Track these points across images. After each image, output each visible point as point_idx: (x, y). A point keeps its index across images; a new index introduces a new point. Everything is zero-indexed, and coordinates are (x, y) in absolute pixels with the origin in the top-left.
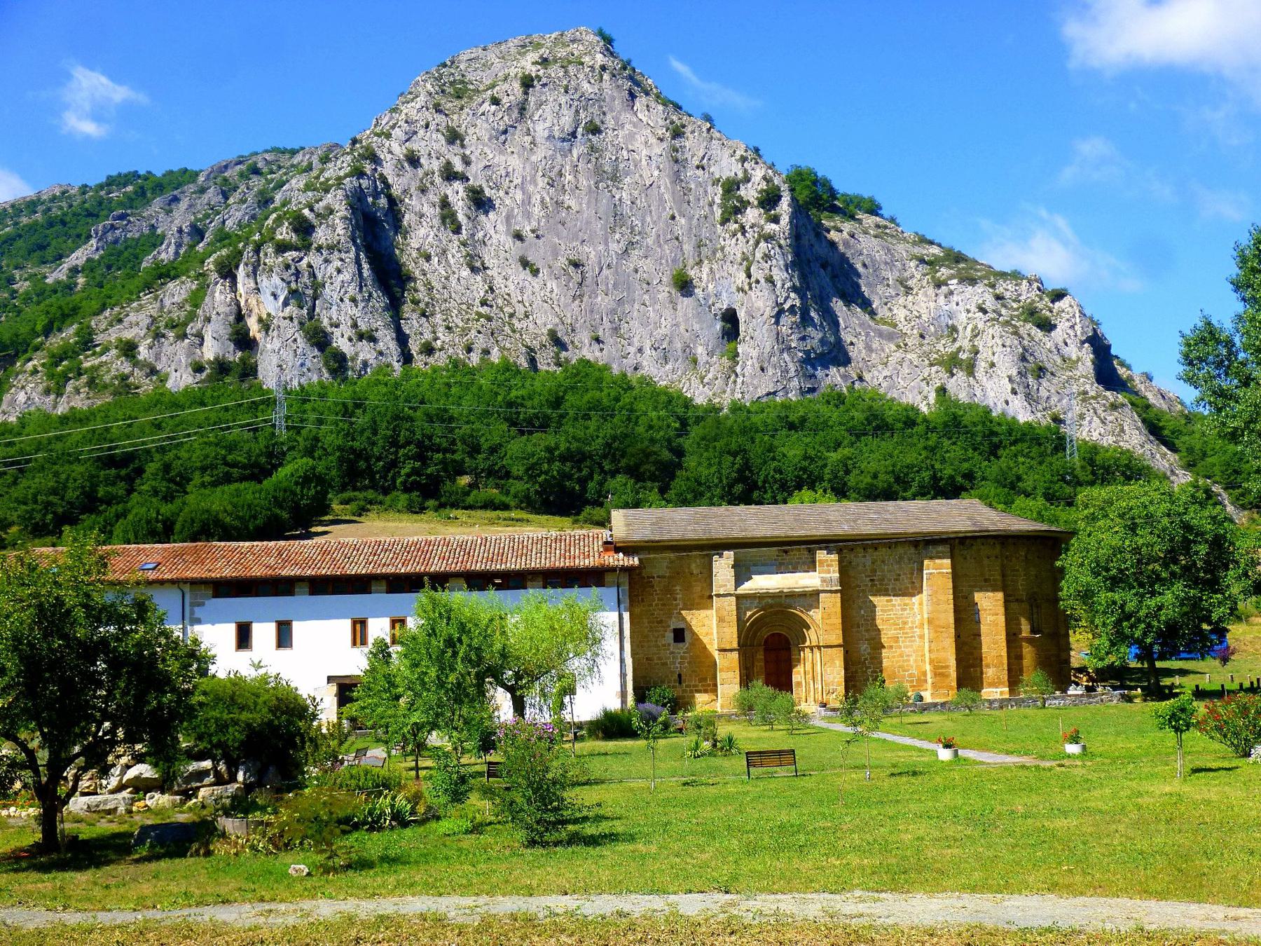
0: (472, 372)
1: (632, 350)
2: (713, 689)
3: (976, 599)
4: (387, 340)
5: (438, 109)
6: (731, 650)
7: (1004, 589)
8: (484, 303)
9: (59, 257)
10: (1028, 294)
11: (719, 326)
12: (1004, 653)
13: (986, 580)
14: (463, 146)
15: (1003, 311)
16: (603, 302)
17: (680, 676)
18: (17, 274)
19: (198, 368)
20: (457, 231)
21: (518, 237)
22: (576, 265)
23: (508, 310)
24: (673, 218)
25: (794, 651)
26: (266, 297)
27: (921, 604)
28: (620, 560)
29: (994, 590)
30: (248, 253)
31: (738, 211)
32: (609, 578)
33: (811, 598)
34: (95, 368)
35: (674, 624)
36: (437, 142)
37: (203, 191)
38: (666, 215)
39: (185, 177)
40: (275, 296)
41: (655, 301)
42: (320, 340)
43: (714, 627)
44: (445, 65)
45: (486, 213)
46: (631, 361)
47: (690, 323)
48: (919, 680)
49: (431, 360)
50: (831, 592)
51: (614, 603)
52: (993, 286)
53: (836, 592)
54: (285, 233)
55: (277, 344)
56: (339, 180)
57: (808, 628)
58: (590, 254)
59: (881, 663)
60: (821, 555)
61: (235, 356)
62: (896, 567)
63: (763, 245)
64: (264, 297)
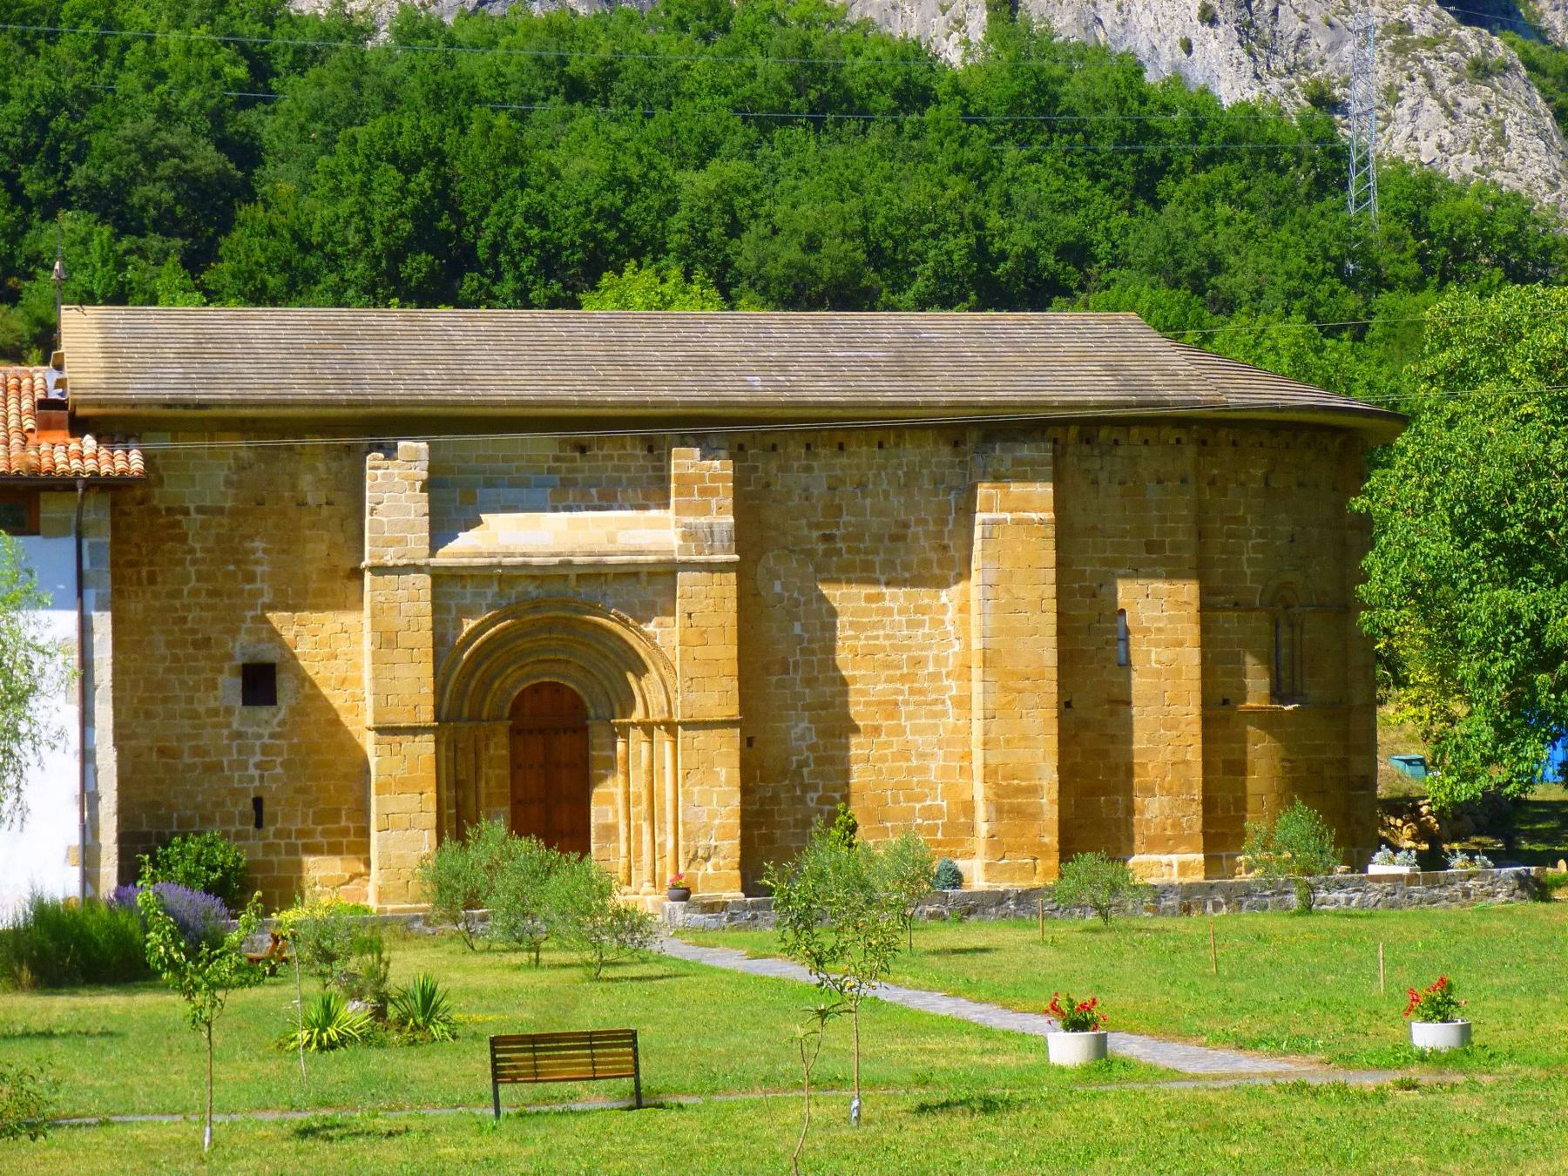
2: (358, 845)
3: (1123, 599)
6: (414, 731)
7: (1200, 572)
12: (1194, 755)
13: (1150, 547)
17: (258, 803)
25: (597, 736)
27: (964, 609)
28: (83, 455)
29: (1170, 576)
32: (52, 508)
33: (650, 583)
35: (242, 647)
43: (363, 661)
48: (950, 827)
50: (710, 567)
51: (68, 585)
53: (724, 567)
57: (641, 669)
59: (847, 774)
60: (685, 461)
62: (897, 502)
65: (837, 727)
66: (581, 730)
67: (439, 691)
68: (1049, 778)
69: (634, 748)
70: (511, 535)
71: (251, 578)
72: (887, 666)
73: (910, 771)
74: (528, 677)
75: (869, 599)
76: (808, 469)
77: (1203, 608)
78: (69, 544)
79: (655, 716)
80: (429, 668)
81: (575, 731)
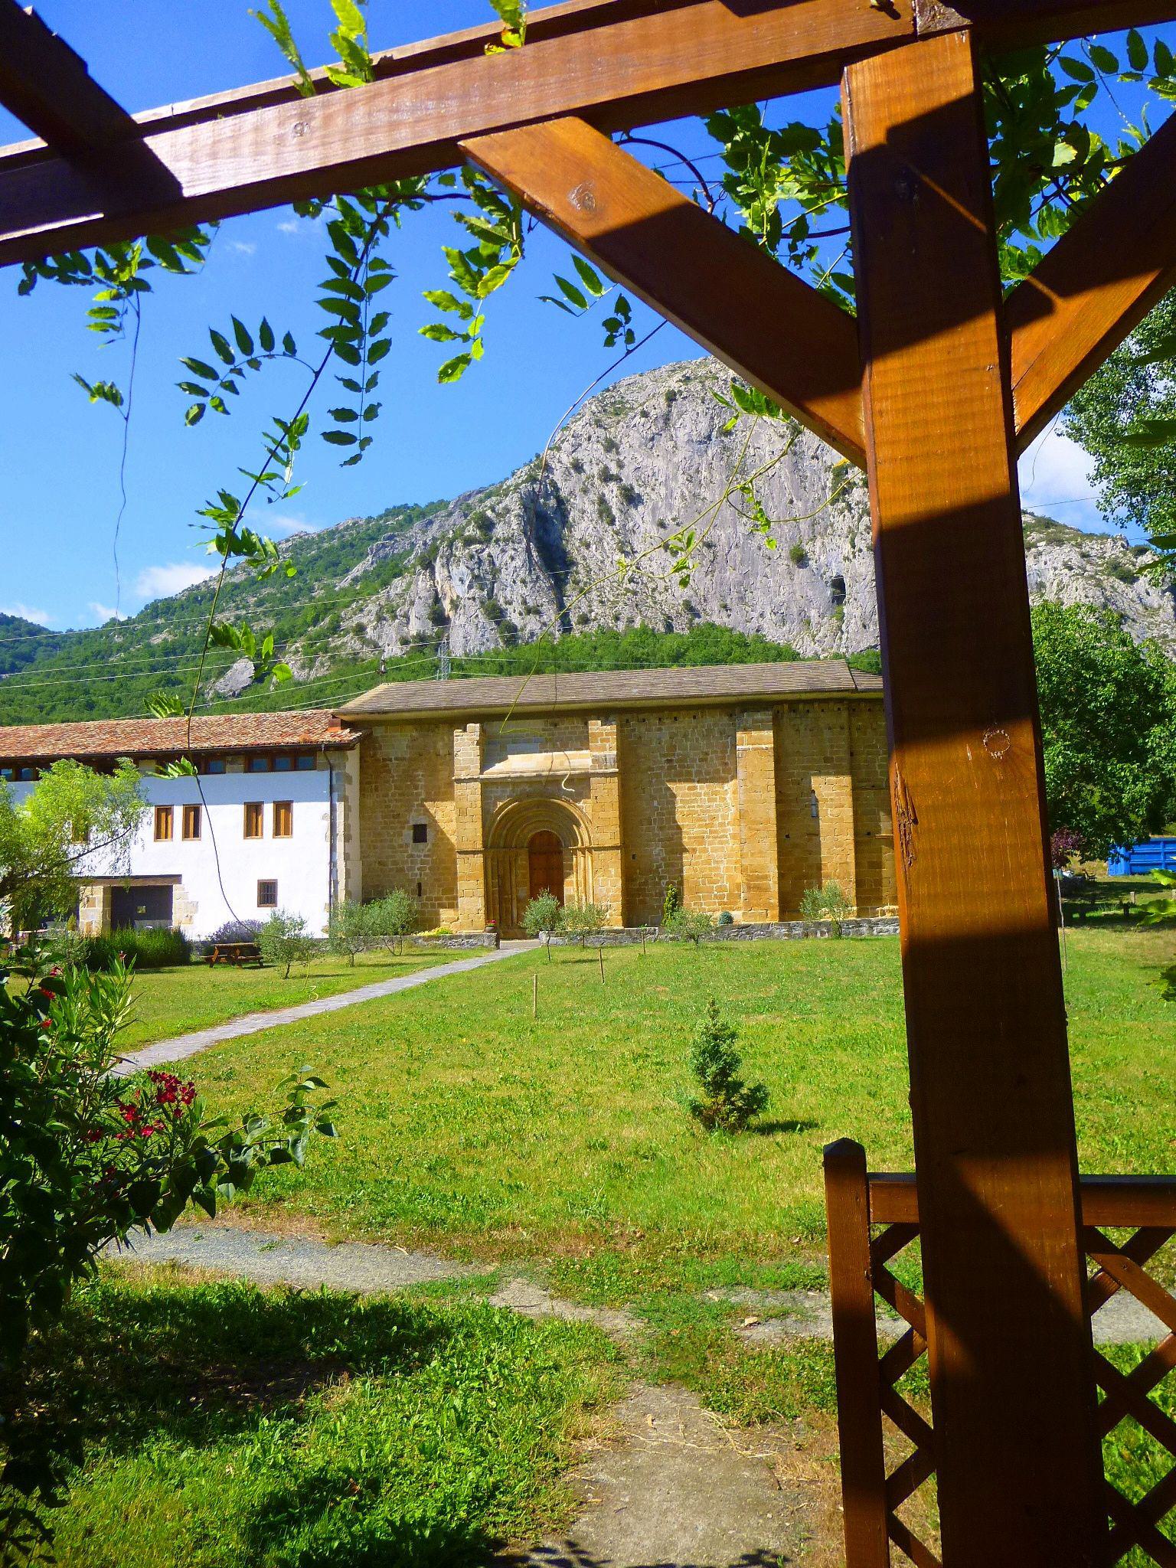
0: (616, 636)
1: (755, 615)
2: (453, 905)
3: (813, 787)
4: (550, 614)
5: (599, 424)
6: (474, 853)
7: (852, 772)
8: (631, 580)
9: (347, 571)
10: (1112, 551)
11: (829, 592)
13: (826, 760)
14: (618, 453)
15: (1088, 567)
16: (731, 575)
17: (419, 885)
18: (316, 585)
19: (405, 642)
20: (612, 522)
21: (662, 525)
22: (709, 546)
23: (651, 585)
24: (791, 502)
26: (456, 582)
28: (346, 735)
29: (837, 774)
30: (443, 548)
31: (845, 491)
32: (321, 759)
33: (581, 782)
34: (336, 648)
35: (415, 818)
36: (598, 449)
37: (450, 514)
38: (785, 500)
39: (443, 504)
40: (461, 580)
41: (775, 573)
42: (496, 614)
43: (458, 819)
44: (608, 390)
45: (636, 507)
46: (754, 625)
47: (805, 590)
49: (586, 629)
50: (605, 775)
51: (326, 791)
52: (1079, 546)
53: (612, 775)
54: (472, 531)
55: (463, 620)
56: (517, 486)
58: (721, 536)
60: (595, 726)
61: (430, 629)
62: (703, 743)
63: (866, 519)
64: (454, 582)
65: (676, 849)
66: (560, 852)
67: (485, 835)
68: (773, 871)
69: (579, 860)
70: (520, 764)
71: (416, 788)
72: (700, 820)
73: (711, 870)
75: (689, 789)
76: (660, 729)
77: (854, 789)
78: (327, 773)
79: (587, 844)
80: (479, 825)
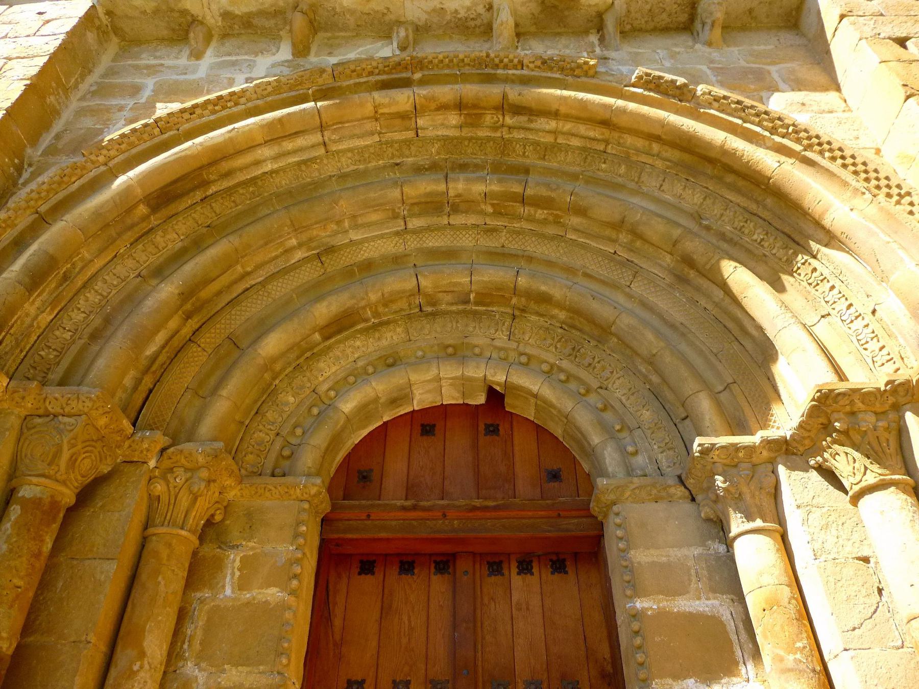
74: (390, 361)
81: (559, 566)
